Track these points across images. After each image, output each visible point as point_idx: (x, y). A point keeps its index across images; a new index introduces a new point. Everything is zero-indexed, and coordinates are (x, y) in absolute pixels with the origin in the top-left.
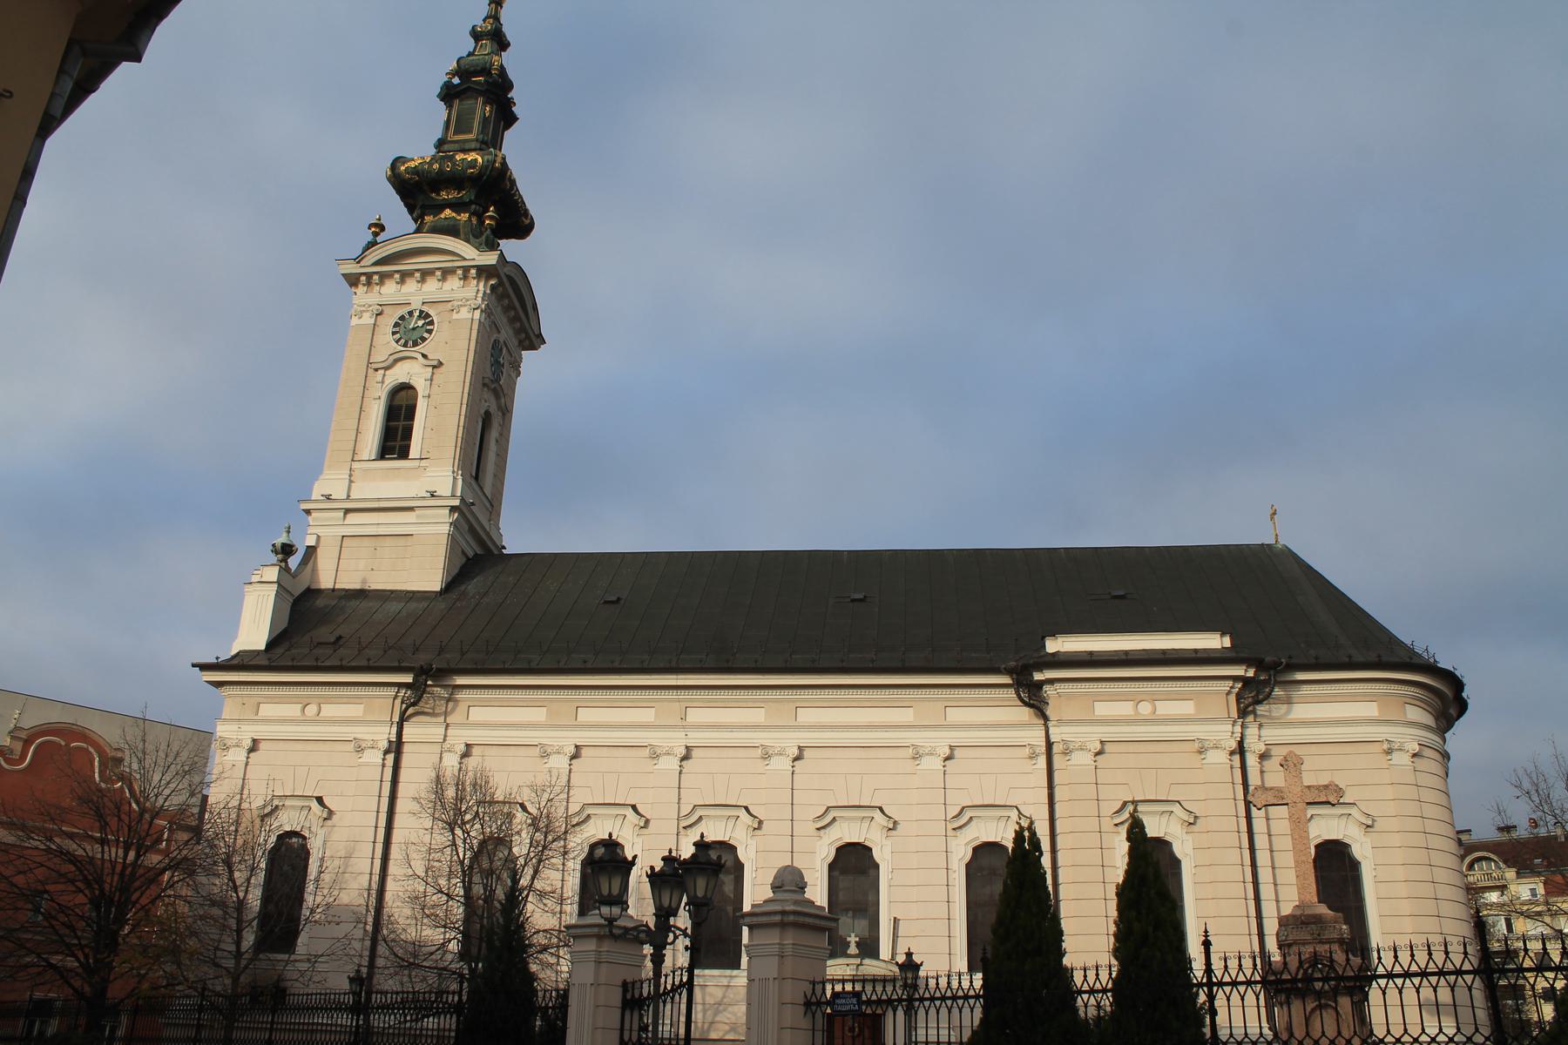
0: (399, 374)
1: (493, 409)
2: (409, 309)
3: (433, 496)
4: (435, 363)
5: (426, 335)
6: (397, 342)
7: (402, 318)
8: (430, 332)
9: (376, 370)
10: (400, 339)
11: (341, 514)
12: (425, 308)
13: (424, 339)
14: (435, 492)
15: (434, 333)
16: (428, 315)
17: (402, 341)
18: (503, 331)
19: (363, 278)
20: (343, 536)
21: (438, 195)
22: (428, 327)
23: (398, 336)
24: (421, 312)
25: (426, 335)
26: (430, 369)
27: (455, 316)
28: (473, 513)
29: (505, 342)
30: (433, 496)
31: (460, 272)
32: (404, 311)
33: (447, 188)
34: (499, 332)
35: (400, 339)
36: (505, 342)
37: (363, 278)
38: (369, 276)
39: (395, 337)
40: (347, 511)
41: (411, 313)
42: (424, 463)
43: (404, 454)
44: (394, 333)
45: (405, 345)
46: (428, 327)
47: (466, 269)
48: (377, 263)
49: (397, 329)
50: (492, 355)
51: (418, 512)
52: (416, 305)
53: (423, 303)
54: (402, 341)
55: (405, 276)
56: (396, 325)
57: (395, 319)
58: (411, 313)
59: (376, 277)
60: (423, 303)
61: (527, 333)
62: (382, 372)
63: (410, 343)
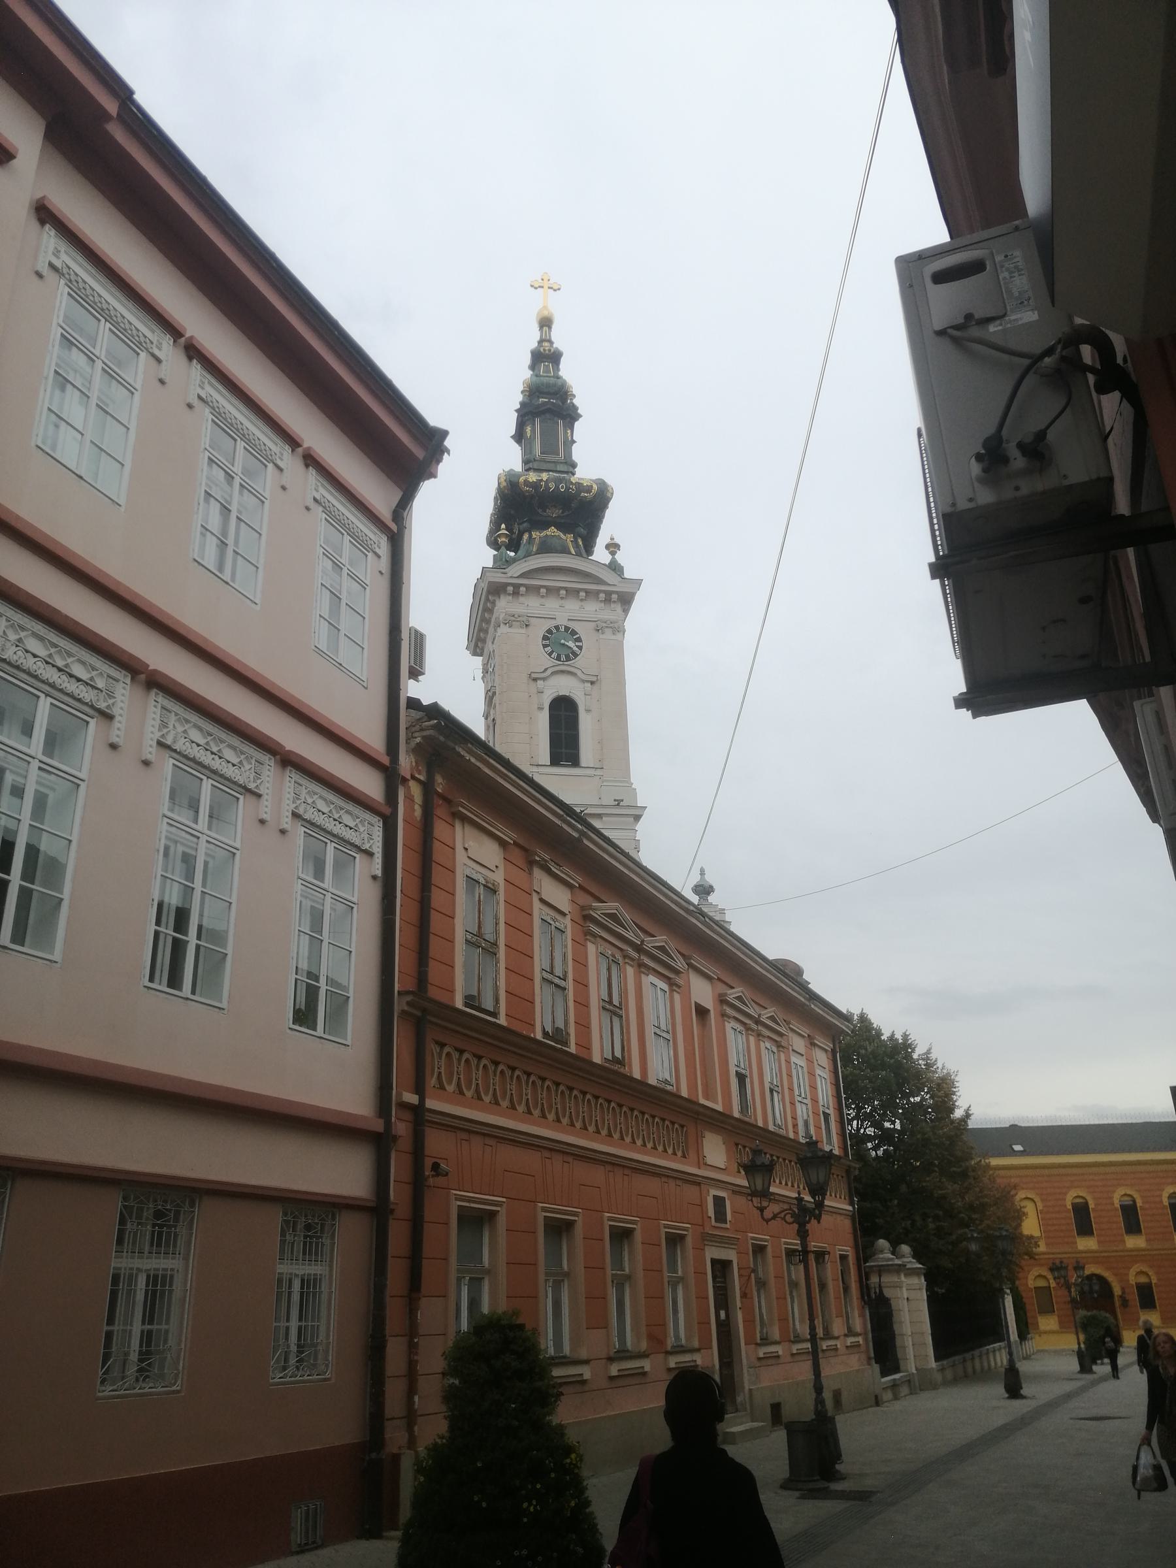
3: (618, 805)
4: (594, 679)
6: (550, 655)
7: (549, 631)
9: (535, 680)
10: (552, 652)
14: (622, 801)
16: (574, 633)
17: (554, 655)
19: (510, 589)
23: (549, 649)
24: (567, 629)
26: (589, 685)
30: (618, 805)
31: (602, 596)
32: (552, 624)
35: (552, 652)
37: (510, 589)
38: (517, 587)
39: (546, 649)
42: (599, 772)
44: (545, 646)
45: (558, 658)
47: (609, 594)
48: (522, 576)
49: (547, 642)
52: (562, 621)
54: (554, 655)
55: (552, 591)
56: (545, 638)
59: (523, 589)
62: (540, 682)
63: (563, 658)
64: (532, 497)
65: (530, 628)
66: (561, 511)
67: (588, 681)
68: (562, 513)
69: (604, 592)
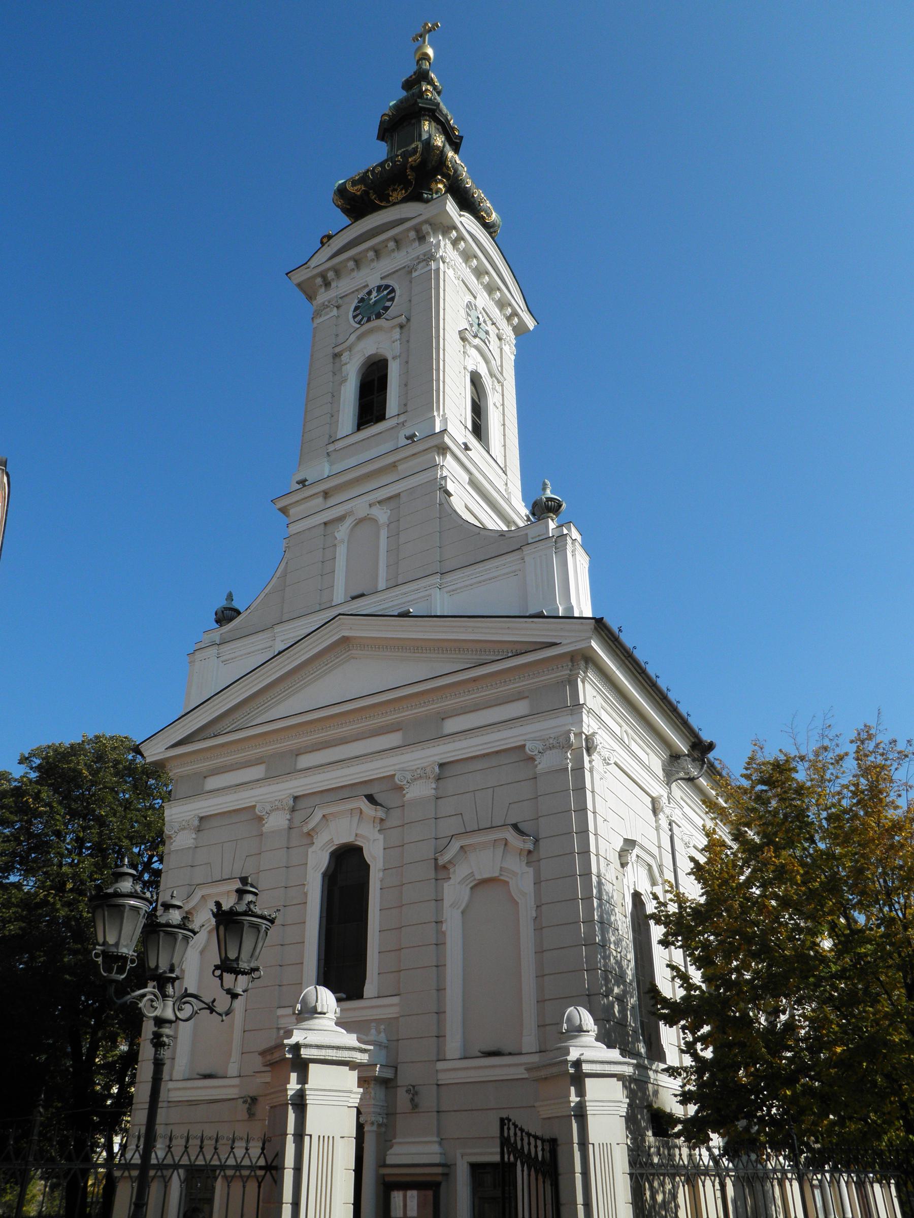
0: (369, 347)
1: (483, 370)
2: (367, 290)
5: (388, 304)
6: (359, 323)
8: (392, 299)
11: (320, 500)
12: (384, 282)
13: (386, 309)
15: (397, 298)
16: (387, 287)
18: (478, 297)
19: (319, 281)
20: (325, 524)
21: (388, 201)
22: (389, 297)
23: (360, 317)
25: (388, 304)
27: (414, 274)
28: (470, 459)
29: (483, 309)
31: (412, 234)
33: (396, 190)
34: (475, 298)
36: (483, 309)
38: (323, 276)
39: (356, 320)
40: (326, 494)
41: (370, 293)
43: (381, 417)
44: (354, 317)
45: (369, 320)
46: (389, 297)
47: (417, 229)
49: (358, 312)
50: (468, 315)
51: (401, 468)
53: (382, 278)
54: (365, 319)
55: (358, 262)
56: (356, 308)
57: (355, 303)
58: (370, 293)
59: (331, 275)
60: (382, 278)
61: (510, 305)
64: (366, 193)
65: (342, 309)
66: (403, 192)
67: (393, 327)
68: (406, 191)
69: (408, 230)
